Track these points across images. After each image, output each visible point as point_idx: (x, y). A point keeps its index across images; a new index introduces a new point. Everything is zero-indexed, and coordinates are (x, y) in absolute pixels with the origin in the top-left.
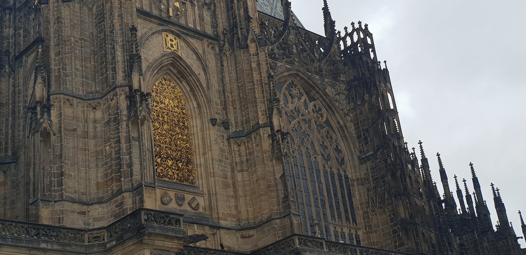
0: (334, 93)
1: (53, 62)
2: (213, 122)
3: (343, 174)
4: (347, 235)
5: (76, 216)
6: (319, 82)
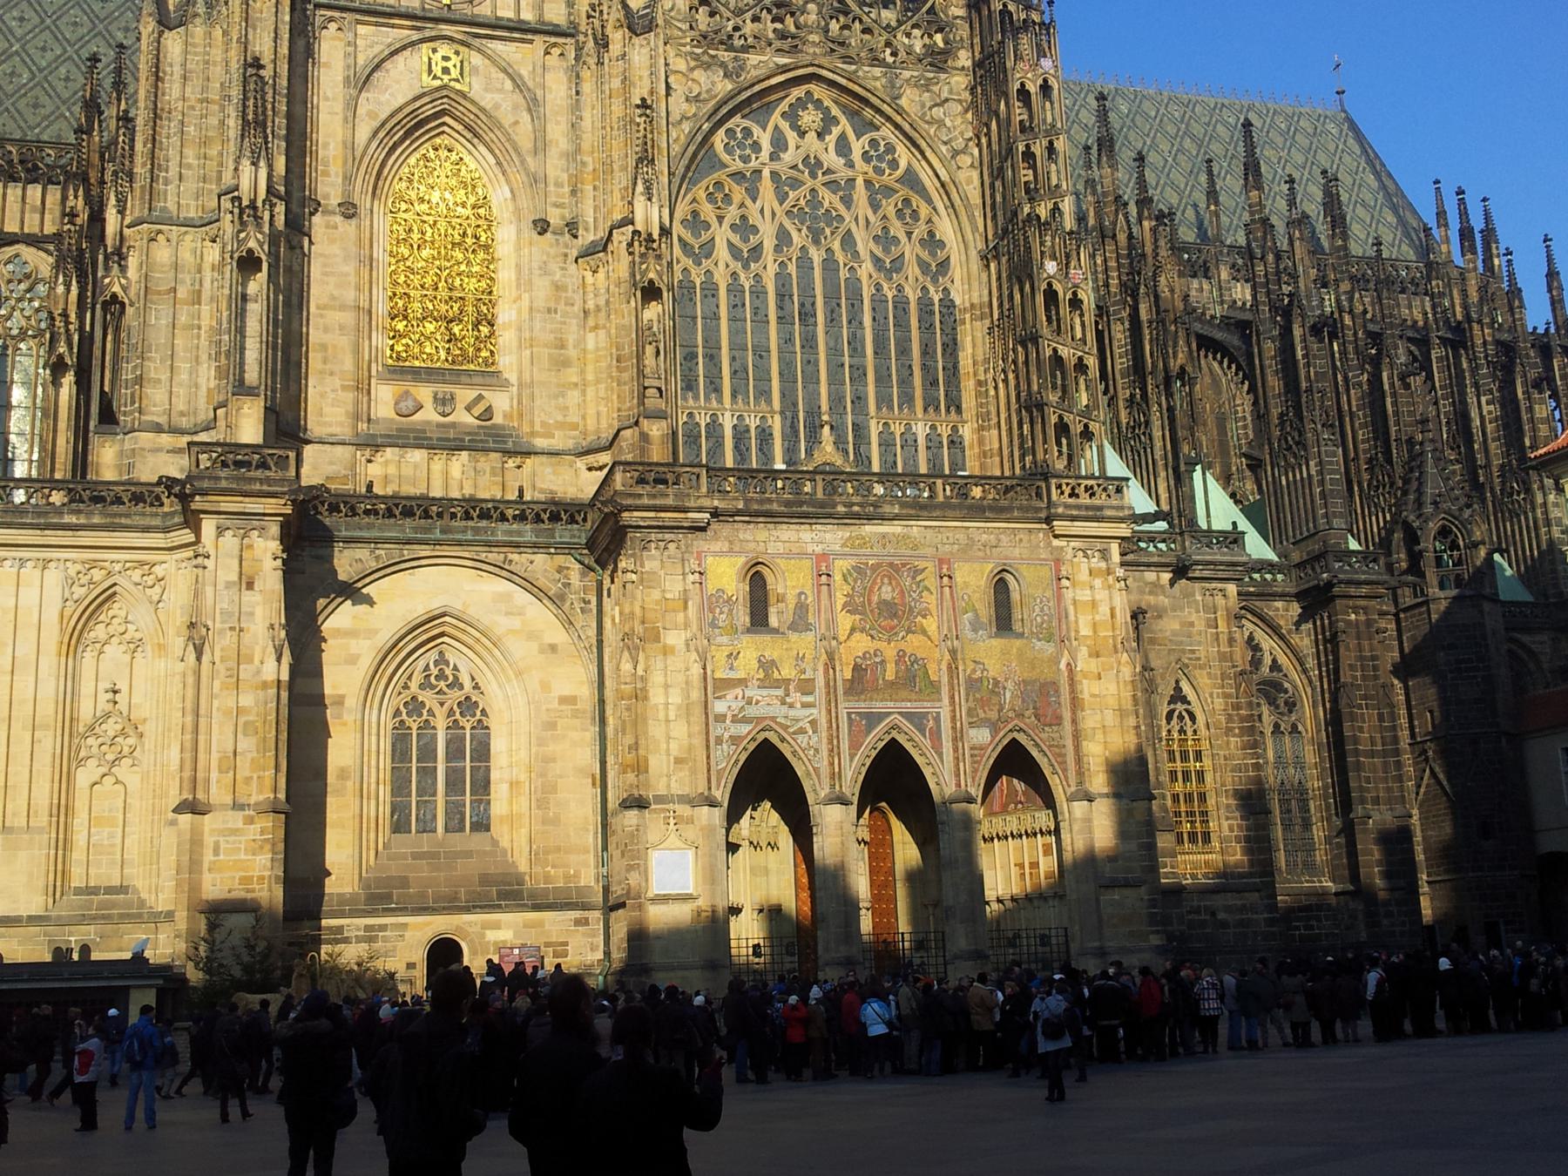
0: (928, 105)
1: (139, 160)
2: (542, 226)
3: (936, 299)
4: (921, 441)
5: (164, 457)
6: (878, 84)
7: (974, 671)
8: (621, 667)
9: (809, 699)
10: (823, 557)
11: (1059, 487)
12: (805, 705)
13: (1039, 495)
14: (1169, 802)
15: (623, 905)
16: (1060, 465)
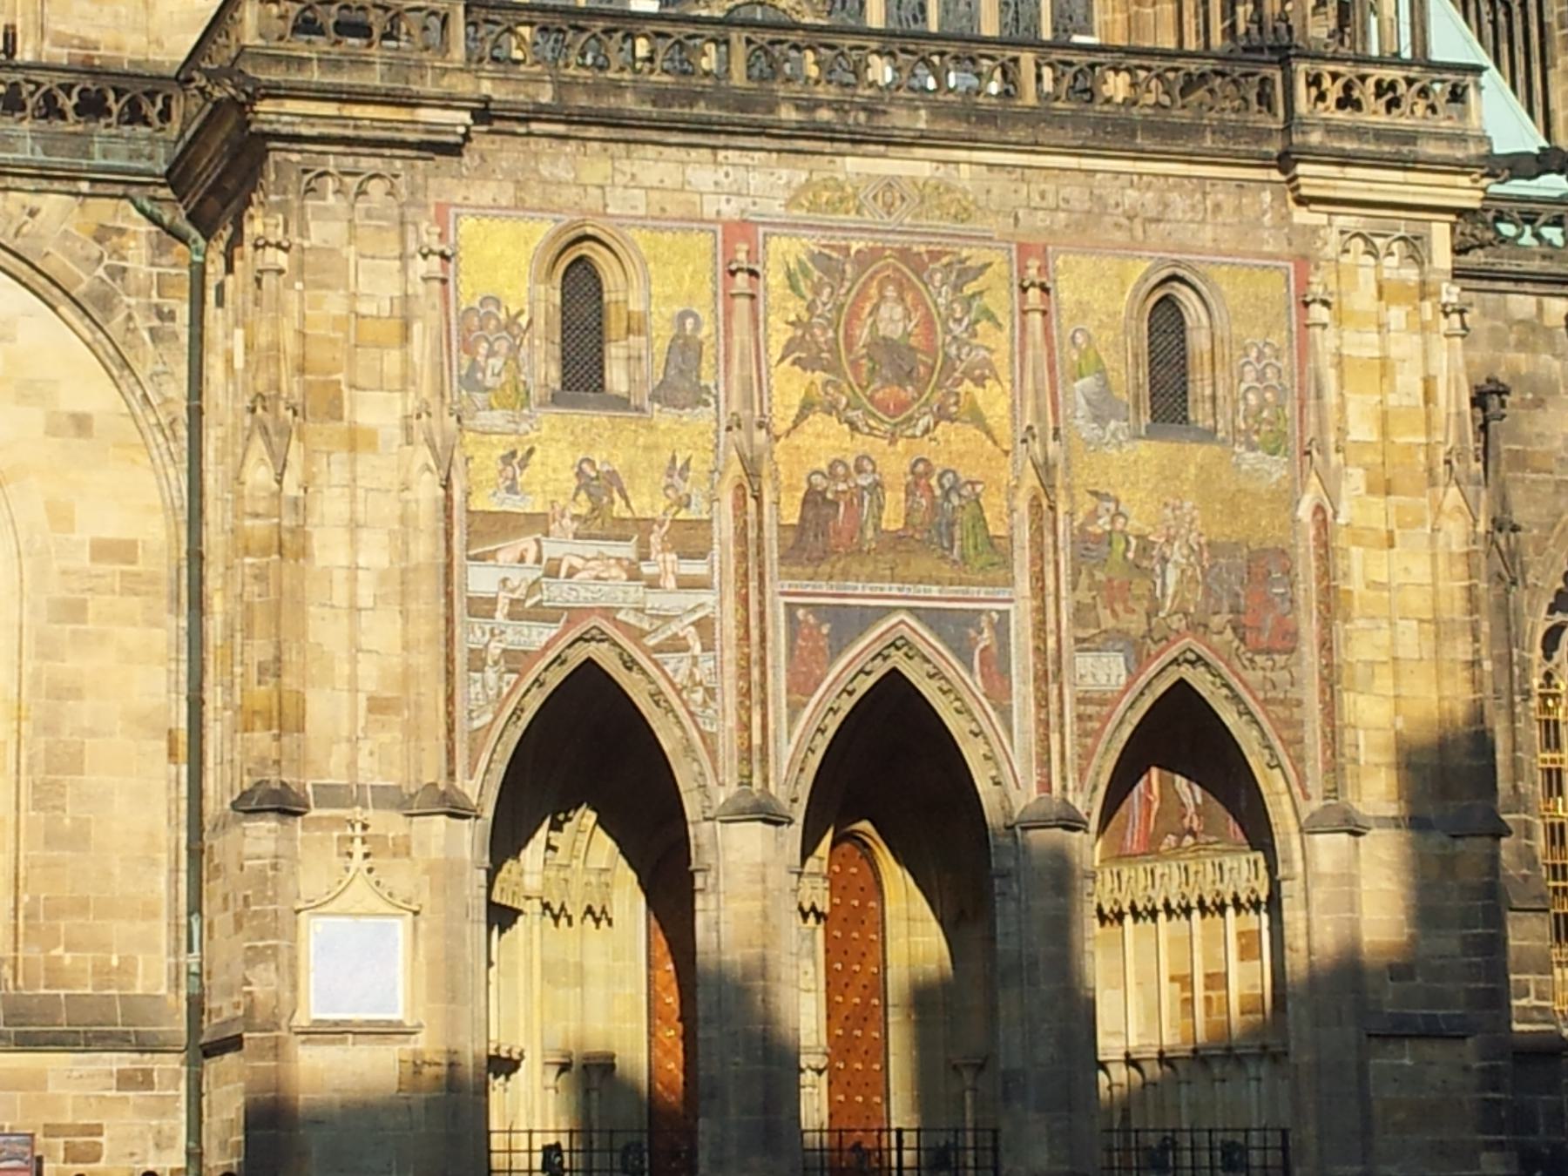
7: (1094, 515)
8: (245, 475)
9: (697, 568)
10: (741, 229)
11: (1315, 81)
12: (686, 584)
13: (1265, 100)
14: (1540, 843)
15: (235, 1043)
16: (1320, 29)
